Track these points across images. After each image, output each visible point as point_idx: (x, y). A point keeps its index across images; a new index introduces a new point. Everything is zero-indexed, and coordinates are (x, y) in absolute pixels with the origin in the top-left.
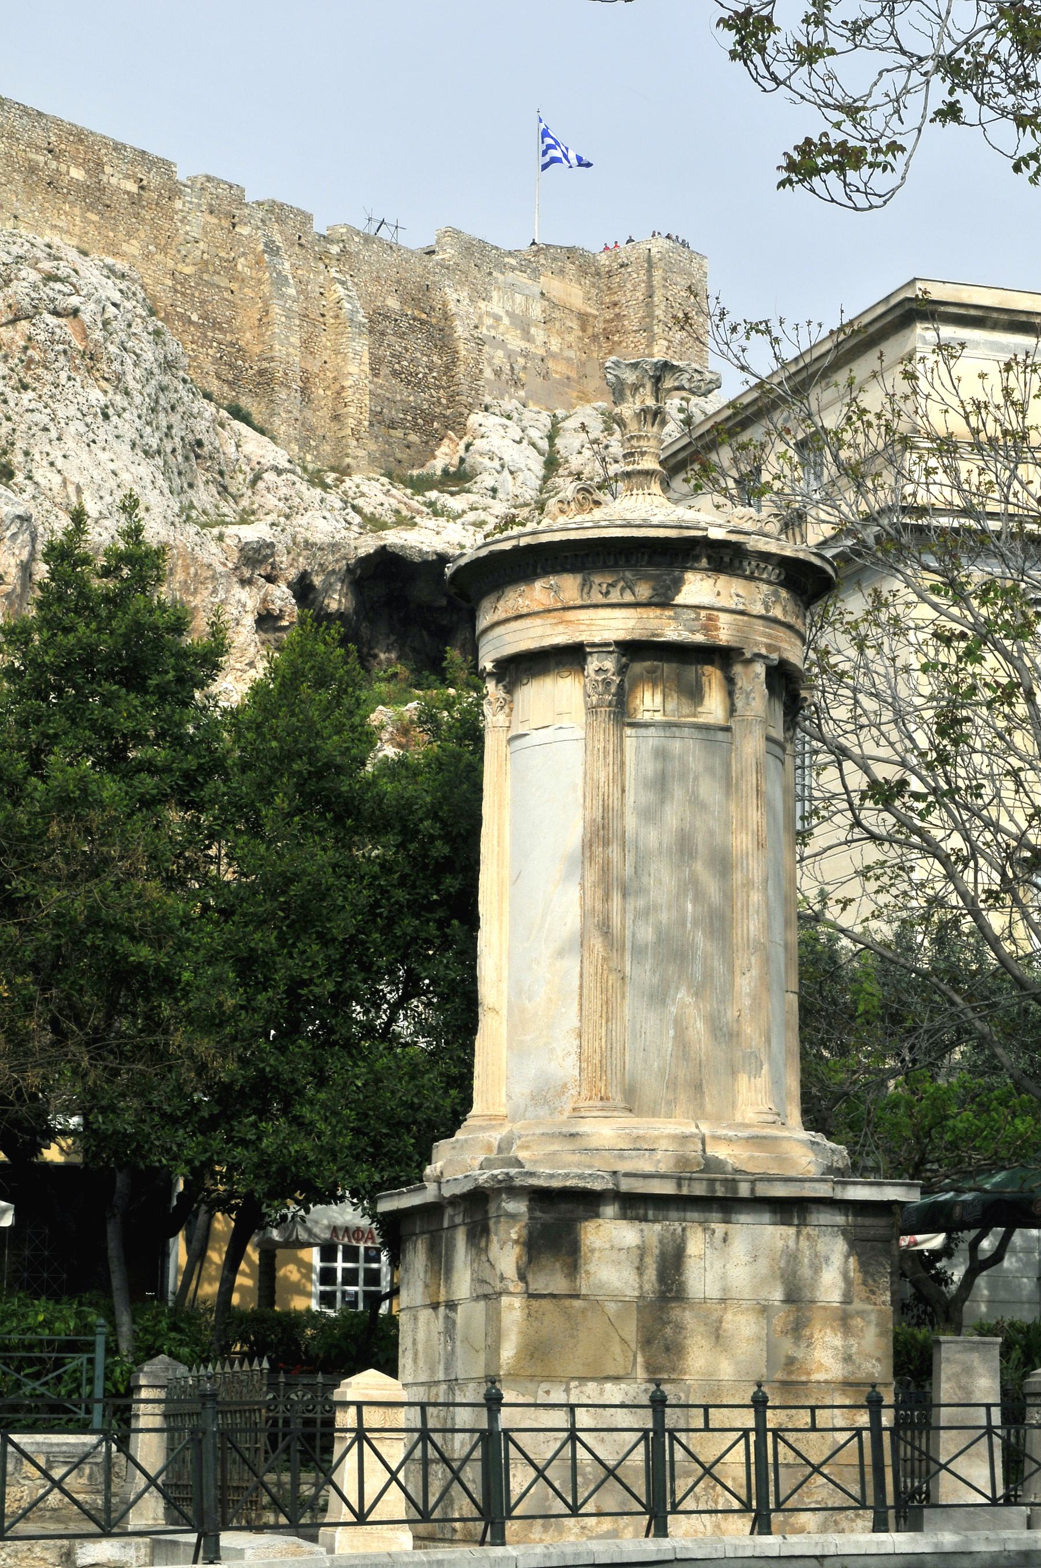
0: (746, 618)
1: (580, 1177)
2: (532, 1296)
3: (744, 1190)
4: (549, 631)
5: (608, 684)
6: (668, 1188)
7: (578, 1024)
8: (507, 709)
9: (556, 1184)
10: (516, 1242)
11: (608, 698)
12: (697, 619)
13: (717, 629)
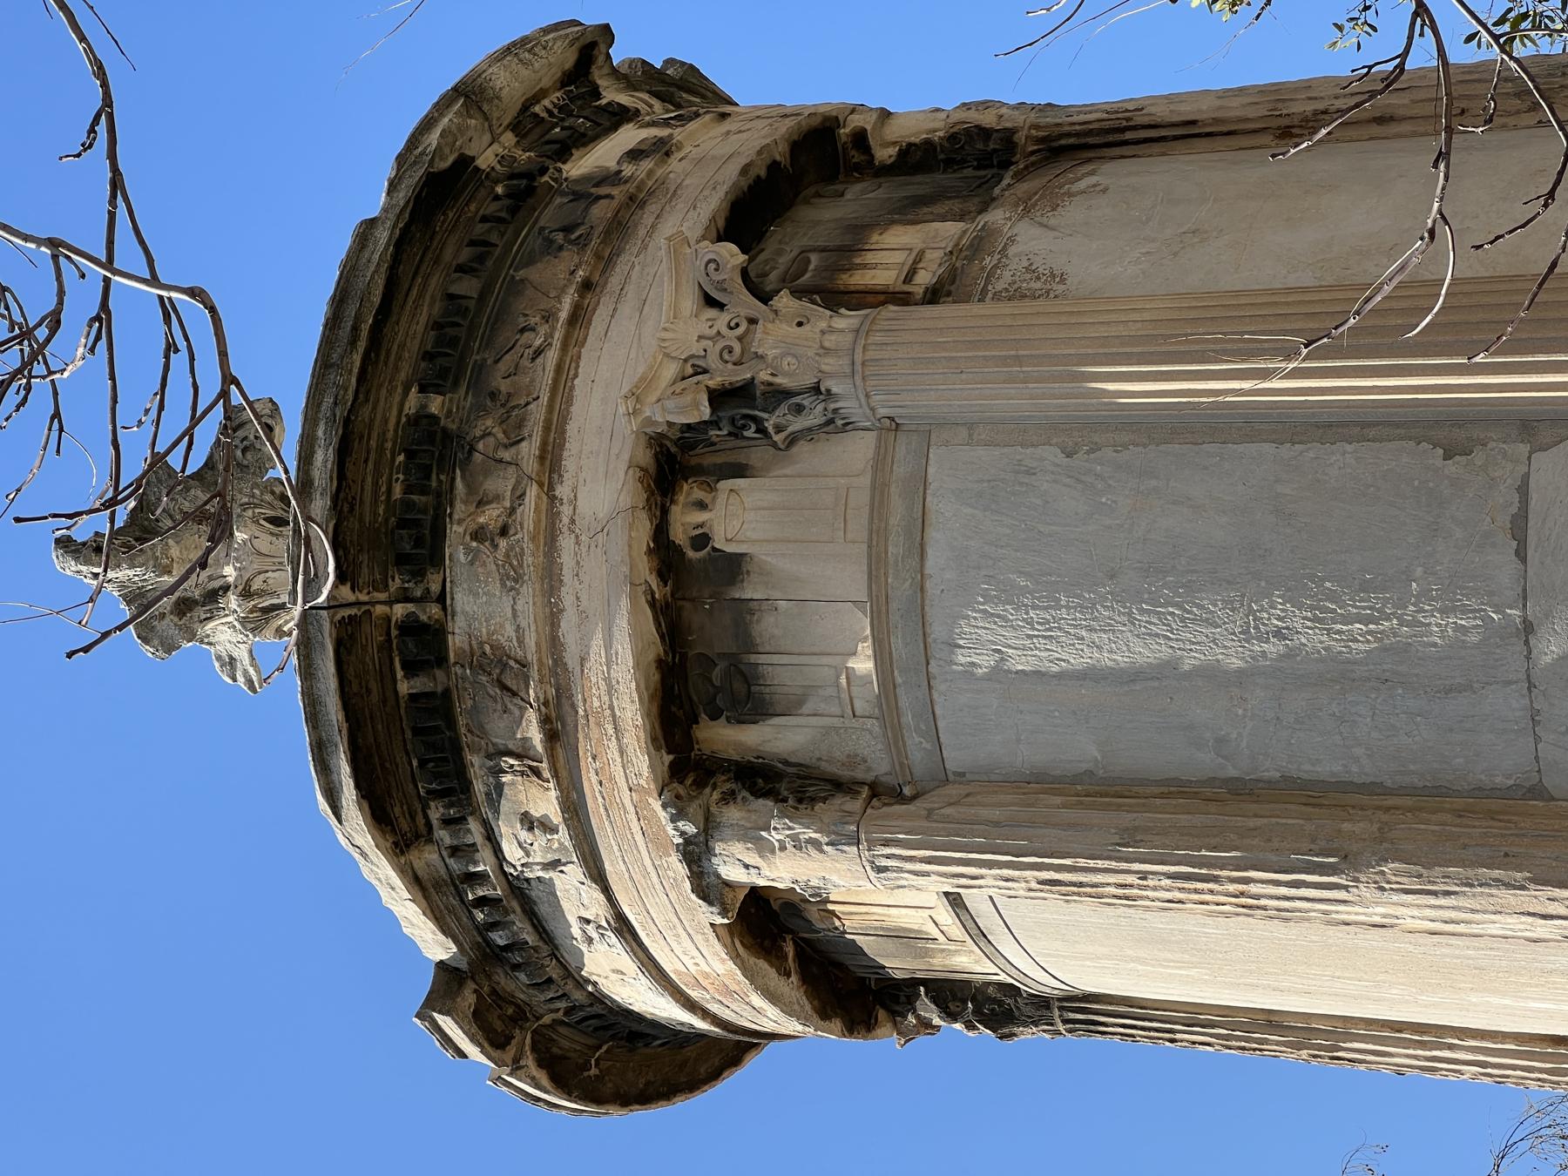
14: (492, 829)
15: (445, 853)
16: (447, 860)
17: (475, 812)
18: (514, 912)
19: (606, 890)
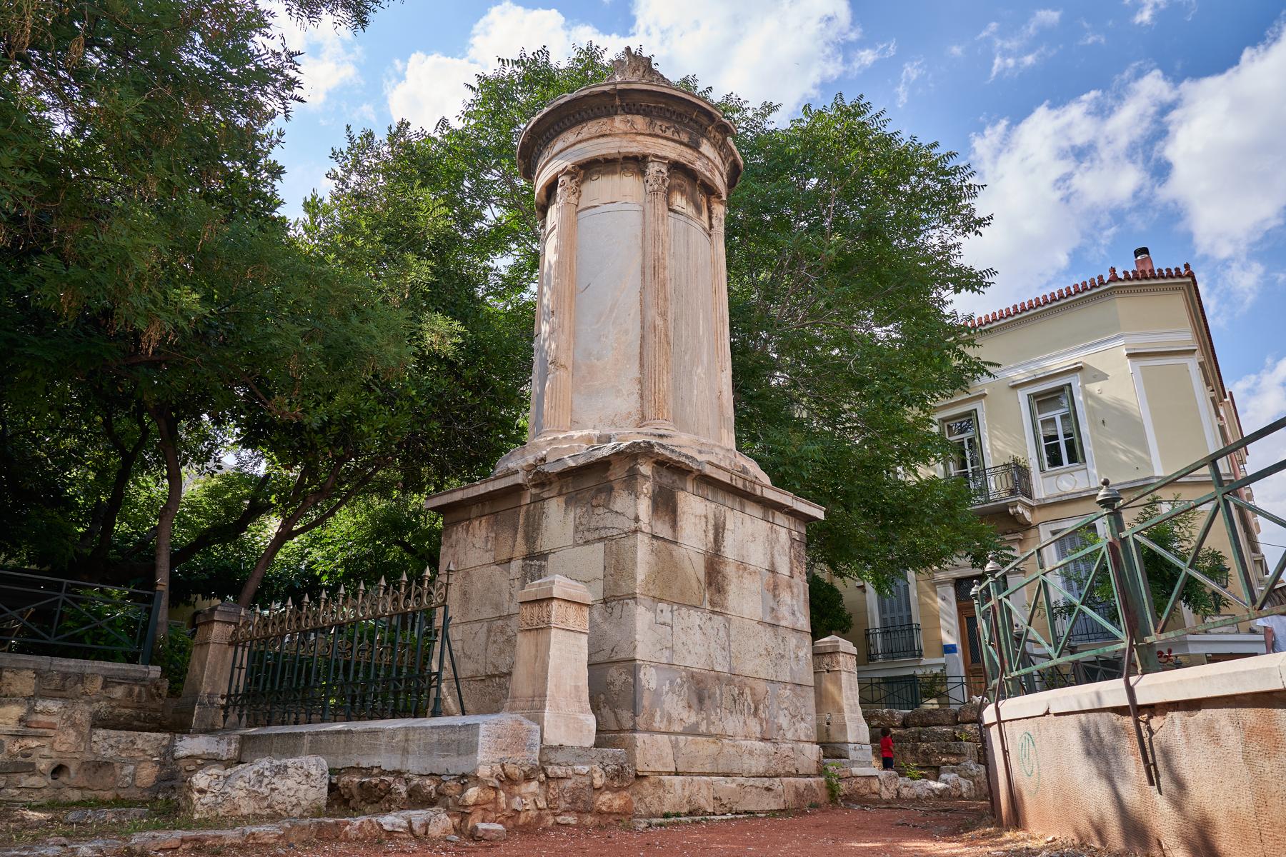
1: (687, 457)
2: (654, 537)
3: (758, 492)
4: (625, 144)
6: (725, 478)
7: (639, 376)
8: (577, 195)
9: (675, 458)
10: (645, 495)
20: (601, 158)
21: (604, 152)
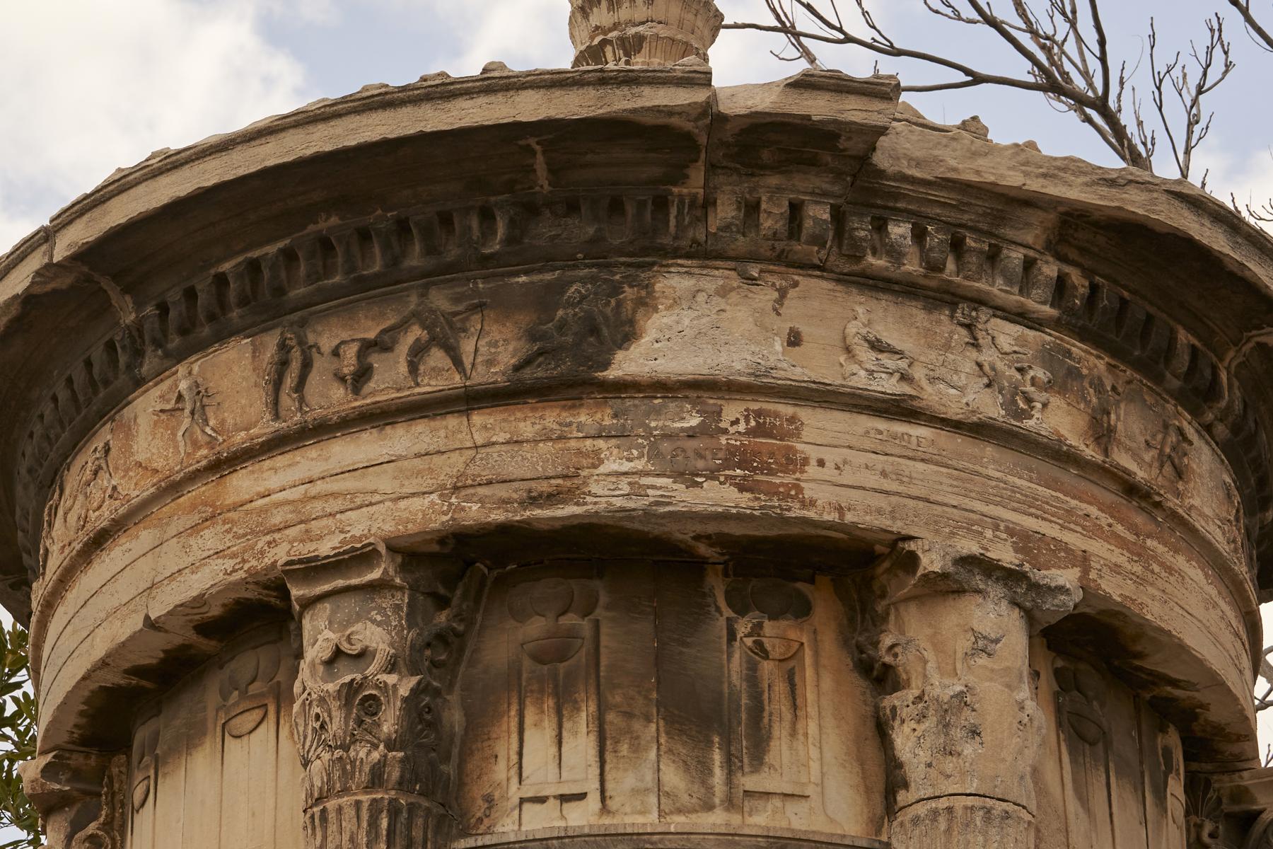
0: (920, 432)
5: (371, 706)
11: (362, 753)
12: (709, 430)
13: (793, 462)
14: (1031, 328)
15: (1031, 253)
16: (1023, 250)
17: (1057, 324)
18: (925, 276)
19: (956, 426)
20: (112, 678)
21: (99, 648)
